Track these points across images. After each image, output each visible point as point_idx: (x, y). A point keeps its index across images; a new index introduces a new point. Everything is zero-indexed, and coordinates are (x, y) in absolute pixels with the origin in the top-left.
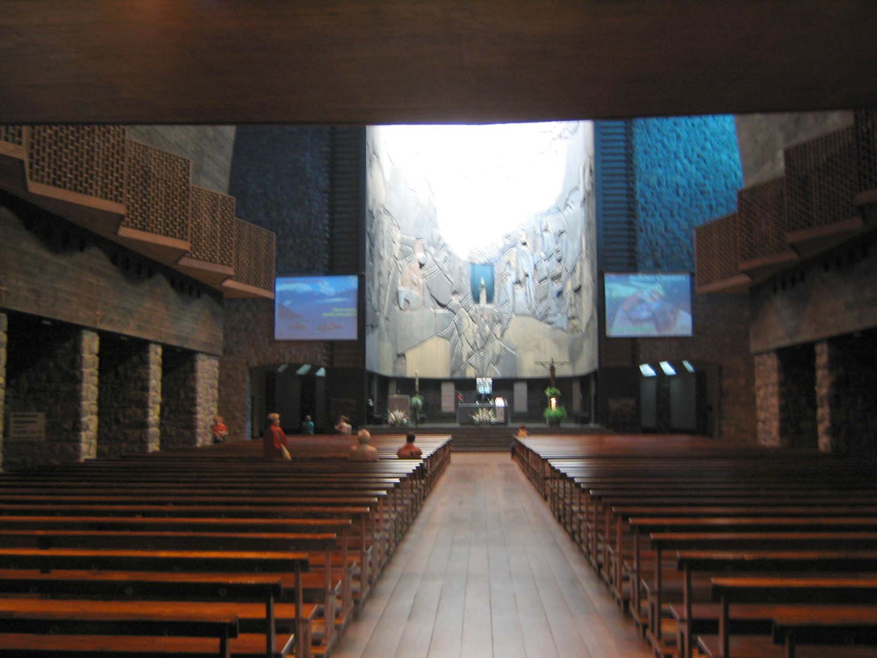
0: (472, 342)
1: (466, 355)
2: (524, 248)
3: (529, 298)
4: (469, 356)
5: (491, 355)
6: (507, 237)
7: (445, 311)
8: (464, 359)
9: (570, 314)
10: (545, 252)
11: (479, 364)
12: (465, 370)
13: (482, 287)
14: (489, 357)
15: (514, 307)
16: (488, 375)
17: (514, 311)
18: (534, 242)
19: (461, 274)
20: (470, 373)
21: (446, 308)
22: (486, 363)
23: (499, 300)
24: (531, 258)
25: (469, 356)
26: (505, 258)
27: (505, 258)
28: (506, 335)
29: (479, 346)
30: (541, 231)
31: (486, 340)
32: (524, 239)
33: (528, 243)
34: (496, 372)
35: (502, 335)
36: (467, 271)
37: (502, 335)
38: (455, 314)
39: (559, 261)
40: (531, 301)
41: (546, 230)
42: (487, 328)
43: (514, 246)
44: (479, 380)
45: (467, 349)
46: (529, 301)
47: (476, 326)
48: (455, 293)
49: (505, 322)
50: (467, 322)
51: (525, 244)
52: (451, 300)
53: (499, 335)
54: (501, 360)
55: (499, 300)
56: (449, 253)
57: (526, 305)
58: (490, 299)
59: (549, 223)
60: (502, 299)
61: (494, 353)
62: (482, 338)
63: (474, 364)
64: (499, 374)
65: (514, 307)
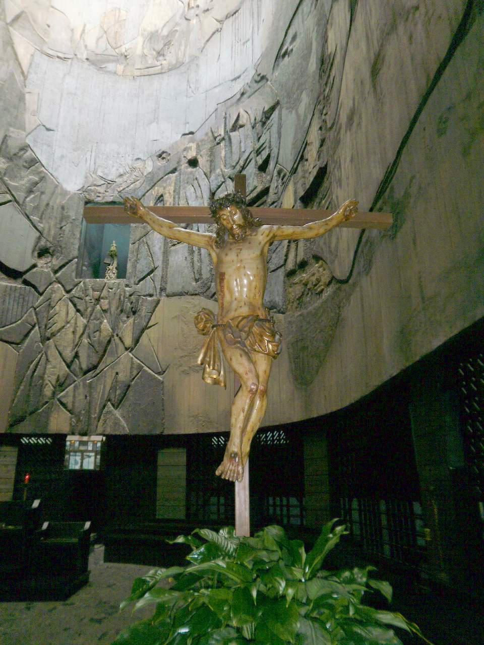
0: (69, 354)
1: (53, 379)
2: (190, 169)
3: (196, 259)
4: (61, 385)
5: (109, 382)
6: (160, 156)
7: (17, 284)
8: (48, 391)
9: (290, 265)
10: (234, 164)
11: (80, 403)
12: (47, 414)
13: (112, 256)
14: (104, 386)
15: (164, 279)
16: (100, 430)
17: (163, 289)
18: (212, 153)
19: (63, 218)
20: (59, 422)
21: (20, 280)
22: (98, 400)
23: (135, 267)
24: (204, 183)
25: (61, 385)
26: (157, 190)
27: (157, 190)
28: (144, 339)
29: (84, 367)
30: (226, 132)
31: (104, 349)
32: (191, 154)
33: (200, 161)
34: (116, 423)
35: (137, 341)
36: (76, 212)
37: (137, 341)
38: (41, 294)
39: (263, 167)
40: (200, 260)
41: (236, 126)
42: (106, 325)
43: (174, 171)
44: (72, 440)
45: (56, 368)
46: (197, 264)
47: (82, 321)
48: (43, 253)
49: (144, 310)
50: (63, 312)
51: (193, 163)
52: (34, 266)
53: (128, 341)
54: (130, 393)
55: (135, 267)
56: (42, 179)
57: (187, 271)
58: (121, 274)
59: (242, 113)
60: (143, 266)
61: (116, 380)
62: (91, 344)
63: (70, 406)
64: (125, 428)
65: (164, 279)
